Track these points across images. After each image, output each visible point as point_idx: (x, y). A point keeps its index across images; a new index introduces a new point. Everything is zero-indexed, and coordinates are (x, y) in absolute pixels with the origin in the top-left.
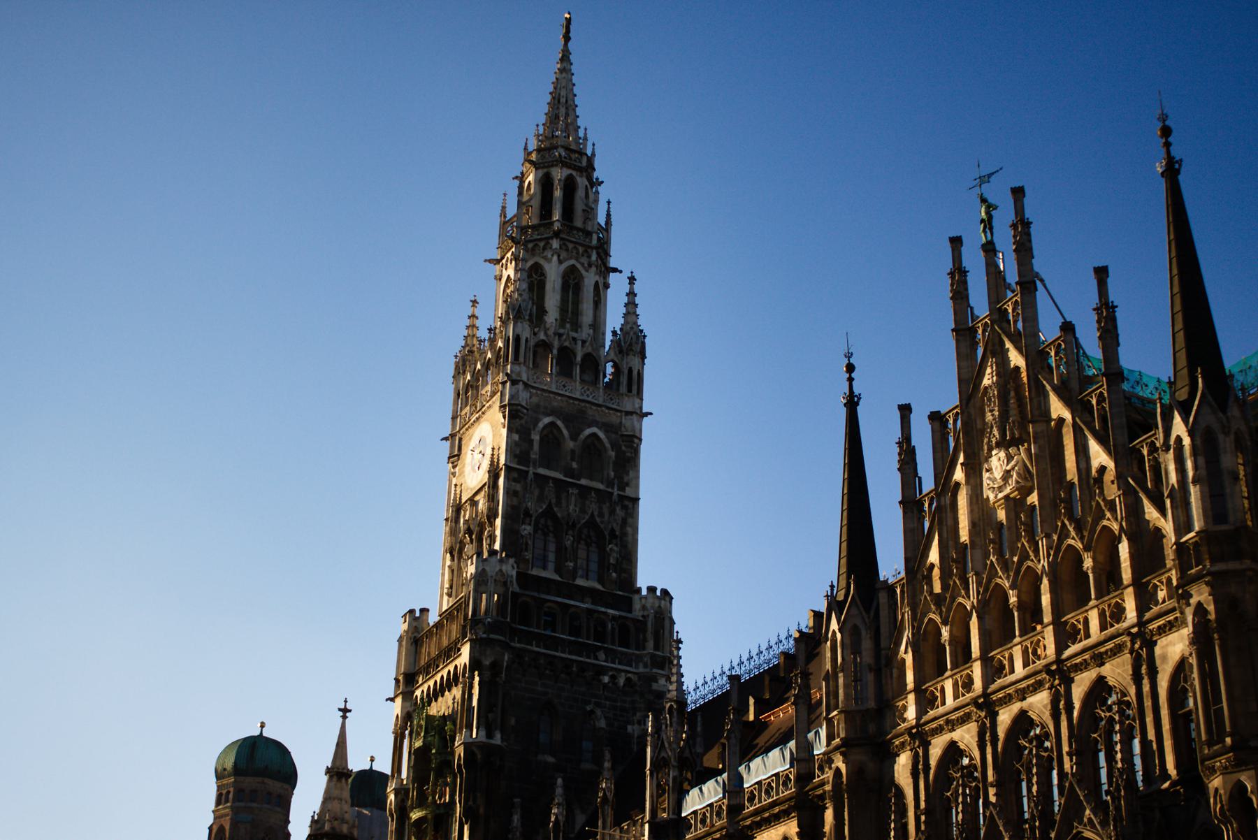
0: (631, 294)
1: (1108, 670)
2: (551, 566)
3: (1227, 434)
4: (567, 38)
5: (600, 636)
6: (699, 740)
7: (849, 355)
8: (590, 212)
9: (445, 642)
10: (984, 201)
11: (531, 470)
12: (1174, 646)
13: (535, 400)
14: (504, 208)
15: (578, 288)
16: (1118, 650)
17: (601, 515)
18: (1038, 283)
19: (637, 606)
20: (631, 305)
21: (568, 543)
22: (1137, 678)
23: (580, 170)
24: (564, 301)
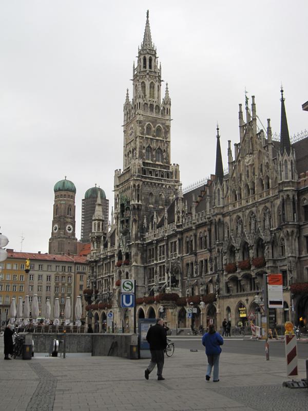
0: (167, 88)
1: (266, 205)
2: (150, 159)
3: (289, 161)
4: (148, 17)
5: (162, 176)
6: (186, 207)
7: (218, 126)
8: (156, 67)
9: (126, 179)
10: (246, 97)
11: (145, 136)
12: (278, 202)
13: (145, 118)
14: (134, 65)
15: (153, 88)
16: (268, 201)
17: (162, 146)
18: (257, 118)
19: (171, 168)
20: (167, 91)
21: (154, 154)
22: (271, 207)
23: (152, 55)
24: (150, 91)
